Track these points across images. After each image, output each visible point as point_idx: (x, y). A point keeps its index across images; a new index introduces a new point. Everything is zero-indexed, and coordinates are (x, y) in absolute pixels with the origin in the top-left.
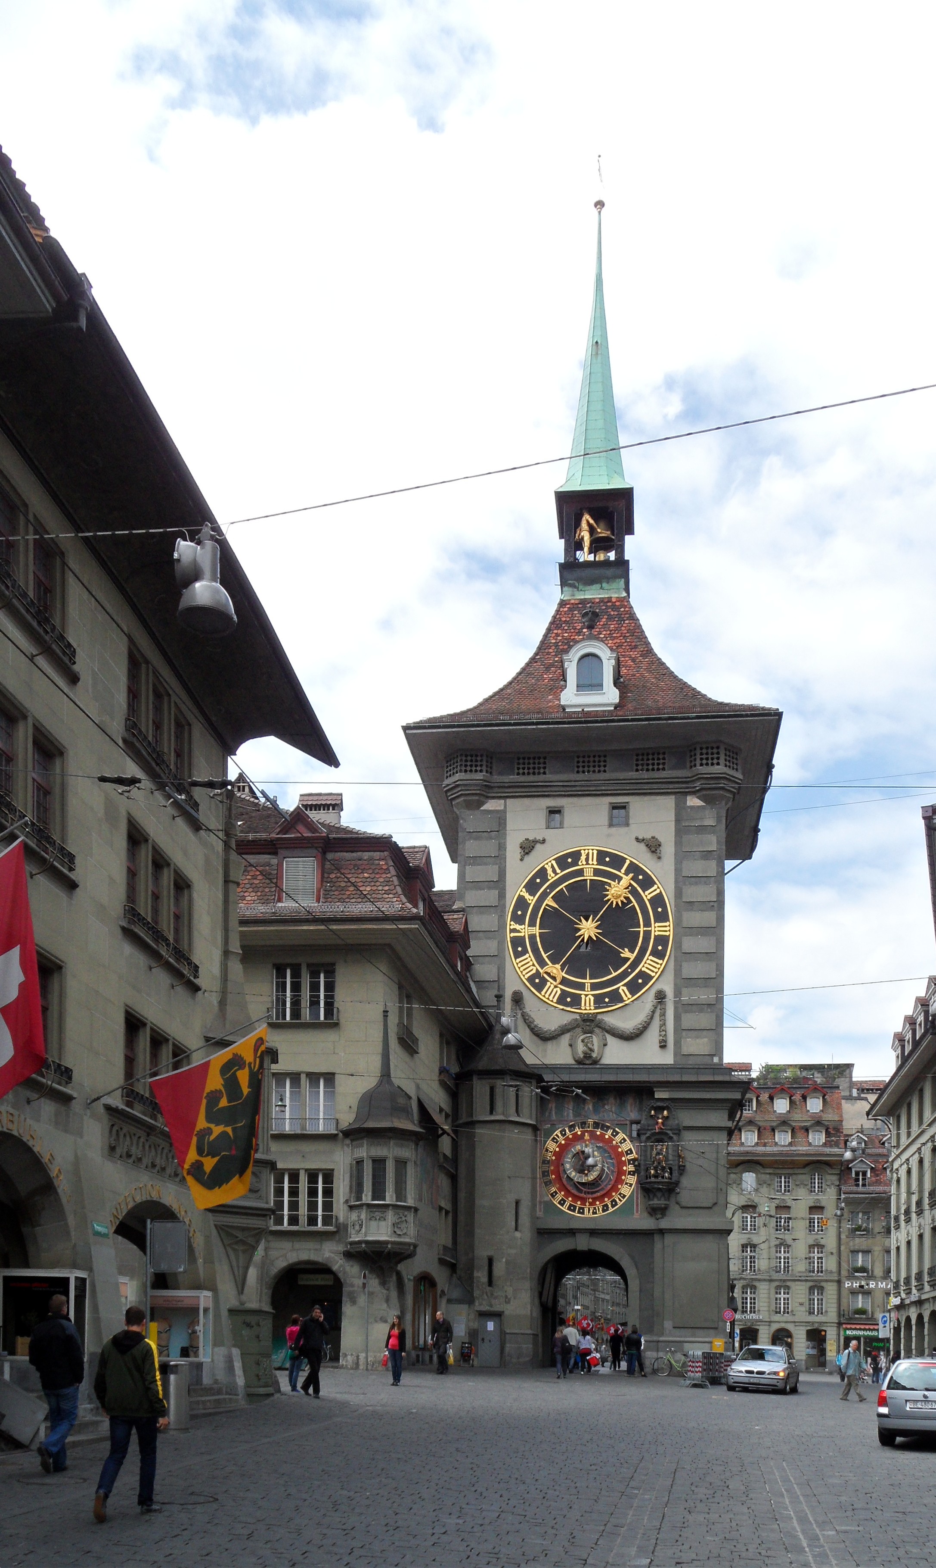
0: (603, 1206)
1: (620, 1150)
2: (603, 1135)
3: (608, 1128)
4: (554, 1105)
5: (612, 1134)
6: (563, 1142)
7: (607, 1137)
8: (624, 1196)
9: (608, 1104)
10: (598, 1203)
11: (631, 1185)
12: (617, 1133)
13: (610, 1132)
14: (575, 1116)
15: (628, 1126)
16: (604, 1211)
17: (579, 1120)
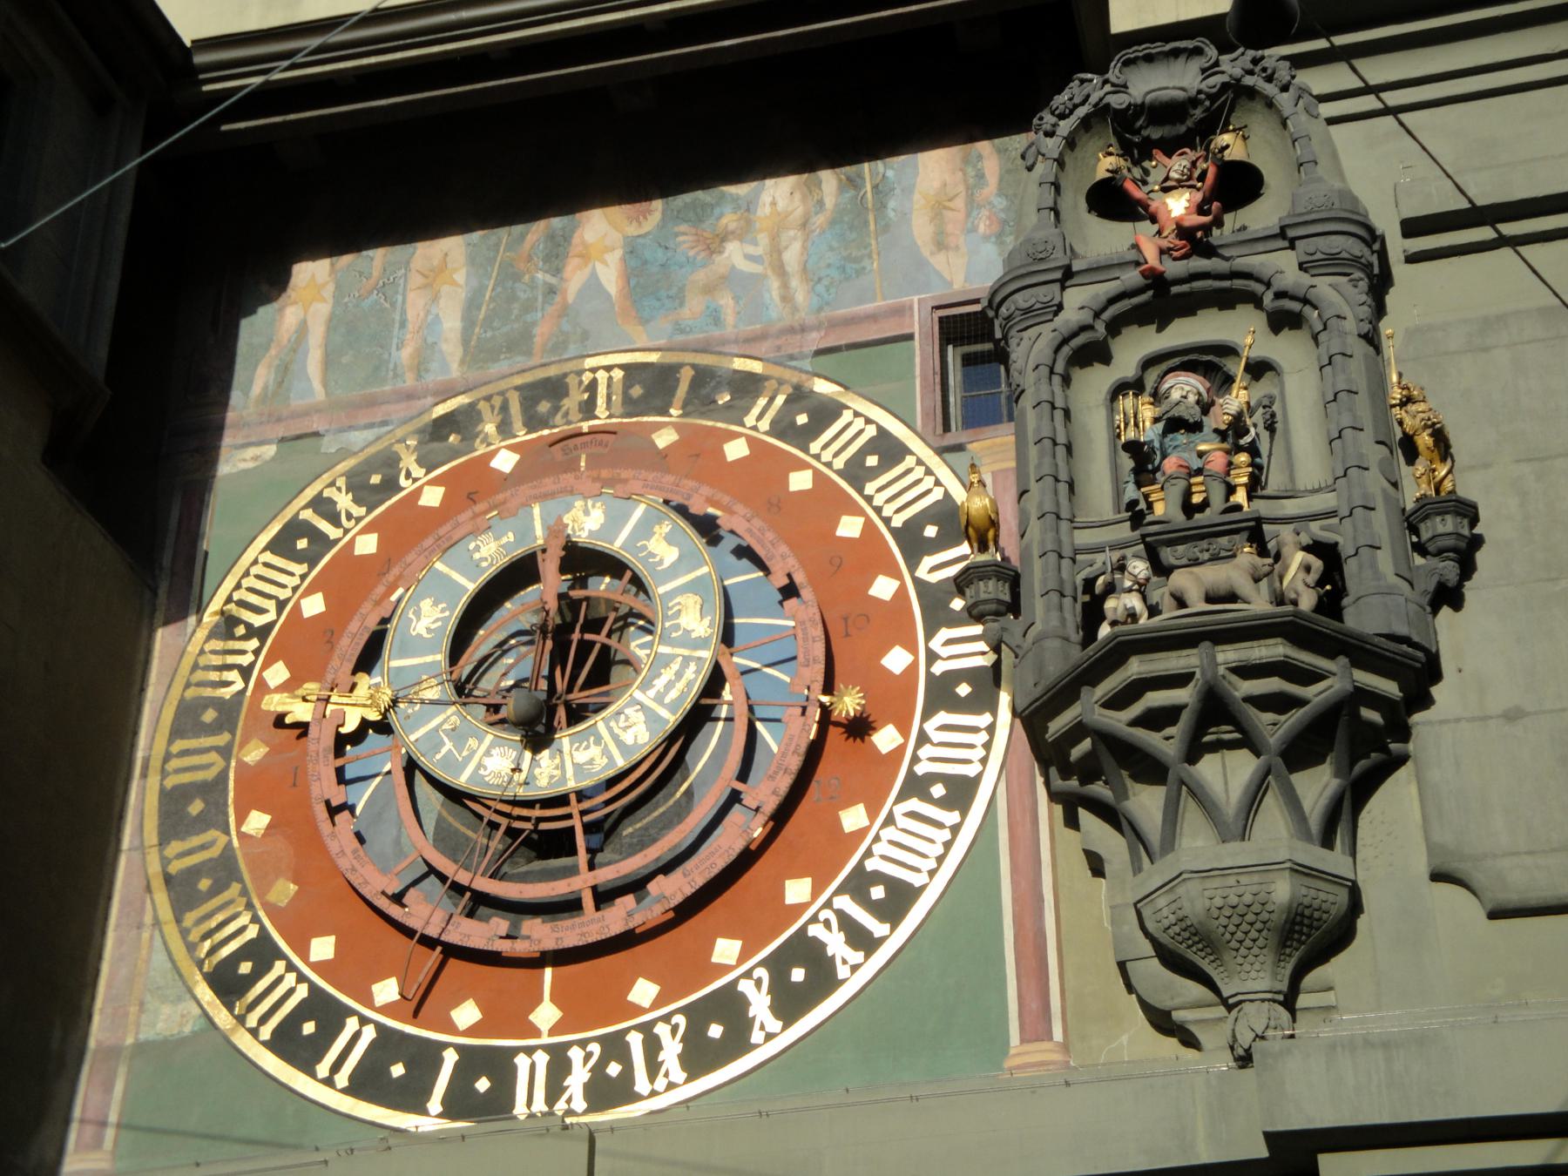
0: (698, 1015)
1: (849, 527)
2: (699, 453)
3: (747, 386)
4: (321, 311)
5: (783, 428)
6: (367, 545)
7: (736, 450)
8: (899, 898)
9: (745, 233)
10: (643, 992)
11: (960, 792)
12: (826, 413)
13: (759, 417)
14: (477, 351)
15: (922, 354)
16: (699, 1057)
17: (513, 373)
